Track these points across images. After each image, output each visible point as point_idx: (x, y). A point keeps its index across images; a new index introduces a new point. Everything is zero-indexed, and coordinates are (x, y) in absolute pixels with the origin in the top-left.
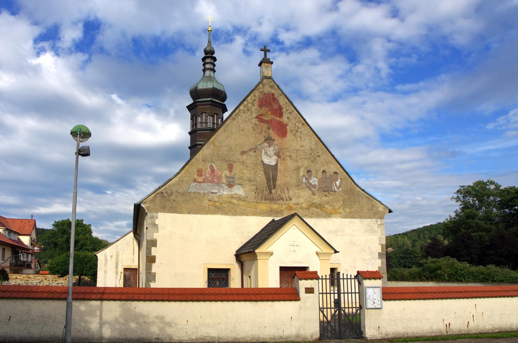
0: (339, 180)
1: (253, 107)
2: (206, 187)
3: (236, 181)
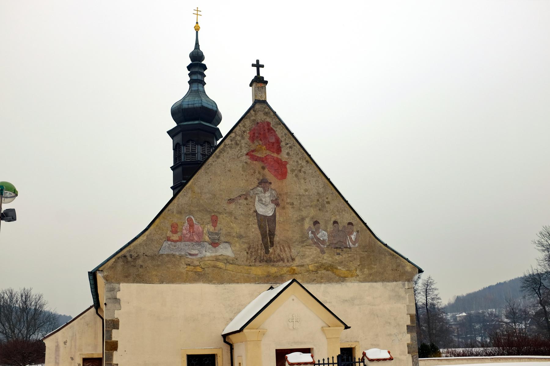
0: (355, 234)
1: (242, 141)
2: (184, 248)
3: (222, 238)
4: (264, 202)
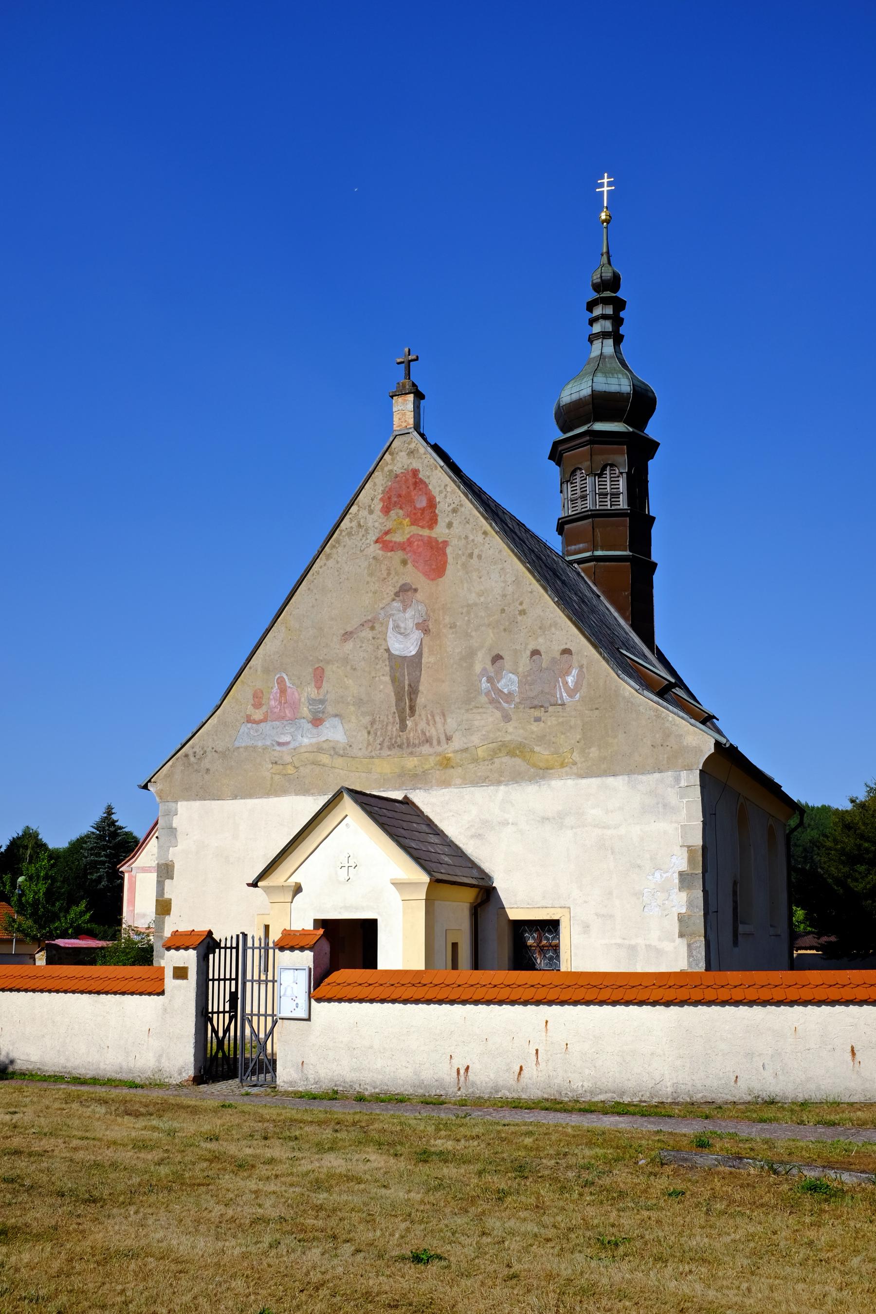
3: (330, 709)
4: (402, 631)
